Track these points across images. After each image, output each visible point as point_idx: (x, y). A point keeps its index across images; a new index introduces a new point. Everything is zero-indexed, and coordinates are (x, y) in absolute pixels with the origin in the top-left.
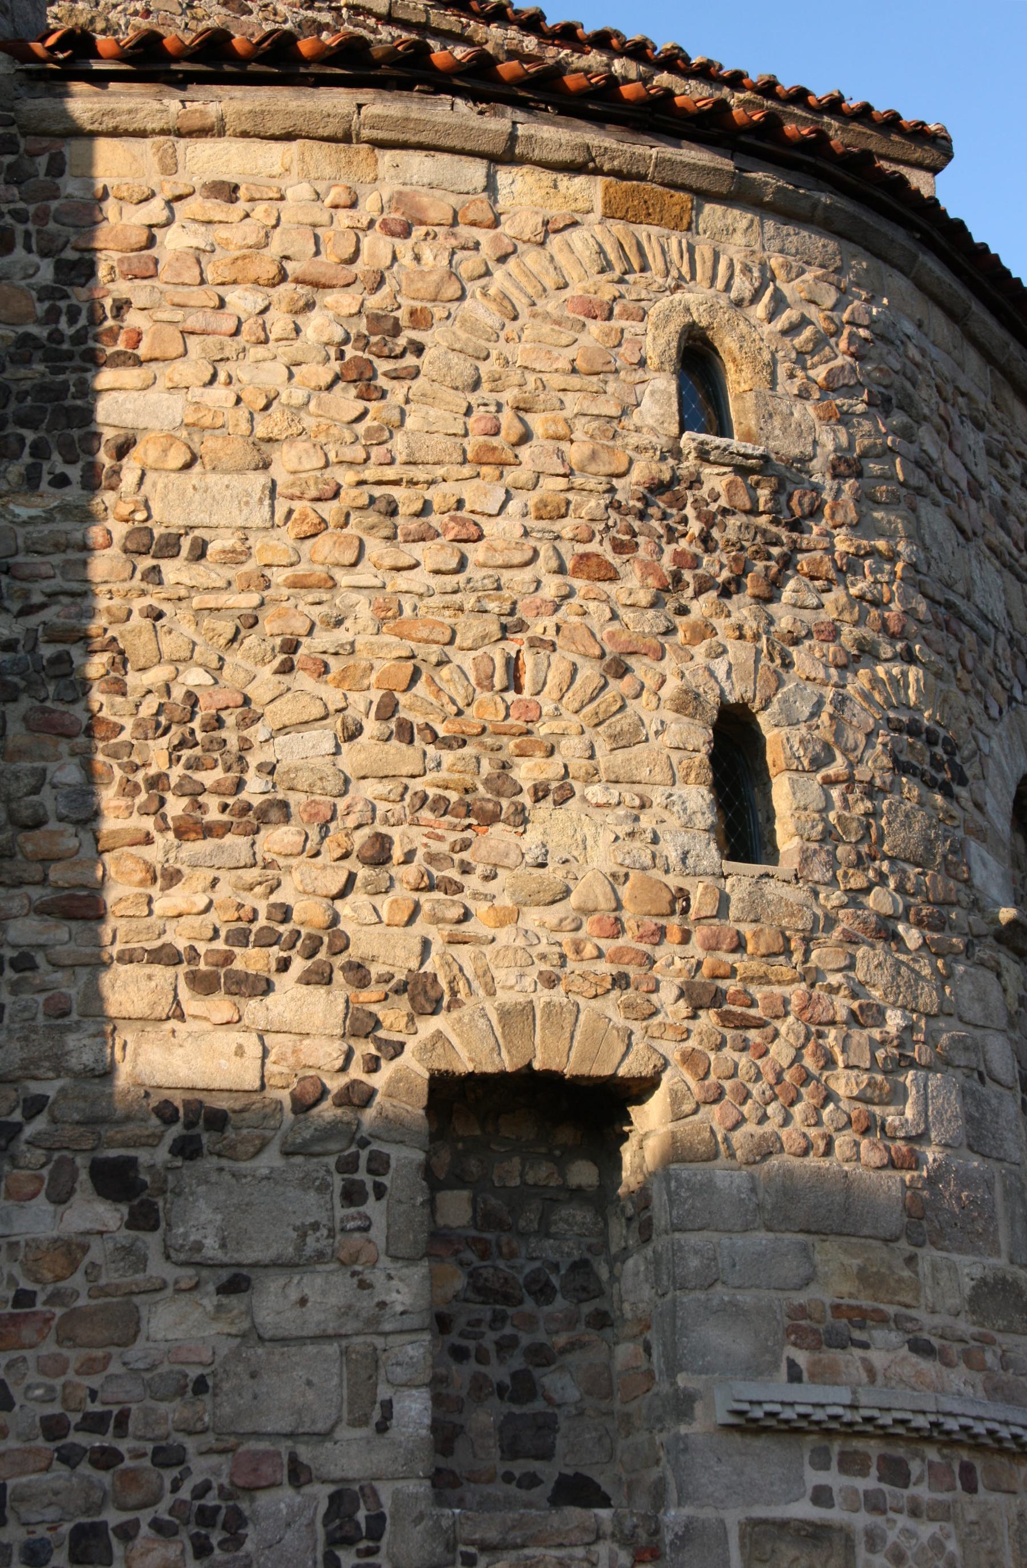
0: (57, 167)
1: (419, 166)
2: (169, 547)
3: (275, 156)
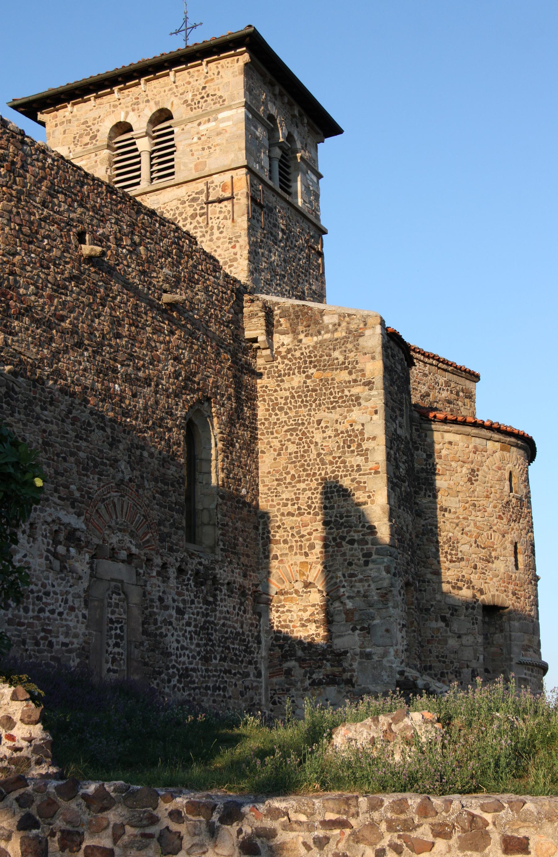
0: (426, 436)
1: (478, 441)
2: (446, 510)
3: (457, 438)
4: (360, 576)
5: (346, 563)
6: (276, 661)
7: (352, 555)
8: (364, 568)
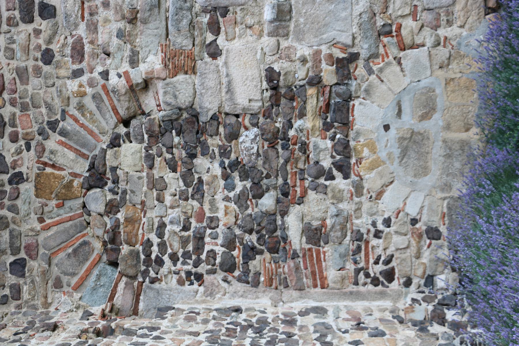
4: (82, 30)
5: (46, 68)
6: (287, 267)
7: (26, 50)
8: (60, 17)
